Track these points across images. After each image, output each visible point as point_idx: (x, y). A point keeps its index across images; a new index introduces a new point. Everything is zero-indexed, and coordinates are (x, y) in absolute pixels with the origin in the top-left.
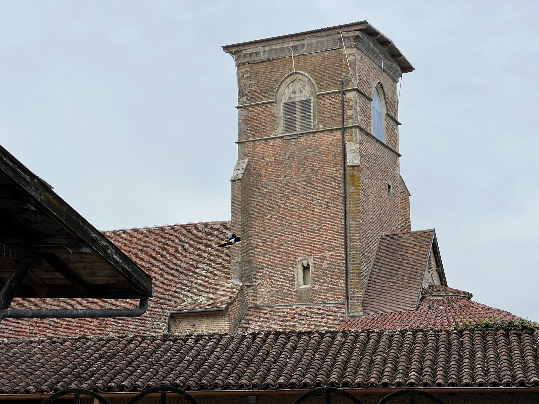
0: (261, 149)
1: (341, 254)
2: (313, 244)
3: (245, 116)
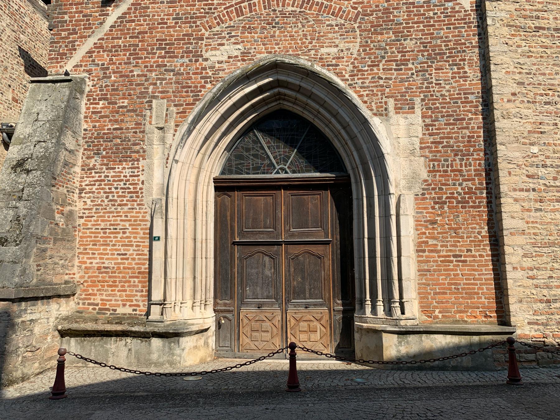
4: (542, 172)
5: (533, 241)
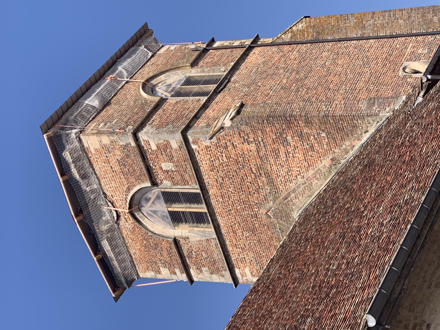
0: (213, 112)
1: (416, 40)
2: (385, 63)
3: (152, 127)
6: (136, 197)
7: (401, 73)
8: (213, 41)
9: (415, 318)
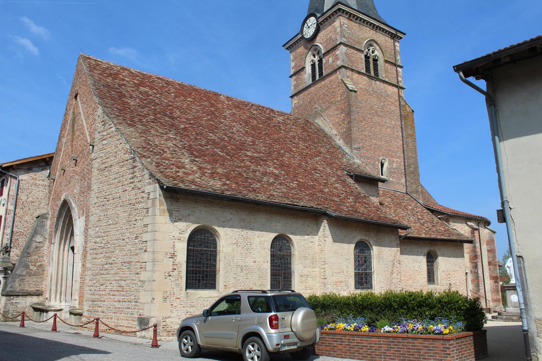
3: (346, 51)
4: (98, 240)
5: (92, 273)
6: (318, 47)
7: (381, 158)
8: (401, 67)
9: (180, 197)
